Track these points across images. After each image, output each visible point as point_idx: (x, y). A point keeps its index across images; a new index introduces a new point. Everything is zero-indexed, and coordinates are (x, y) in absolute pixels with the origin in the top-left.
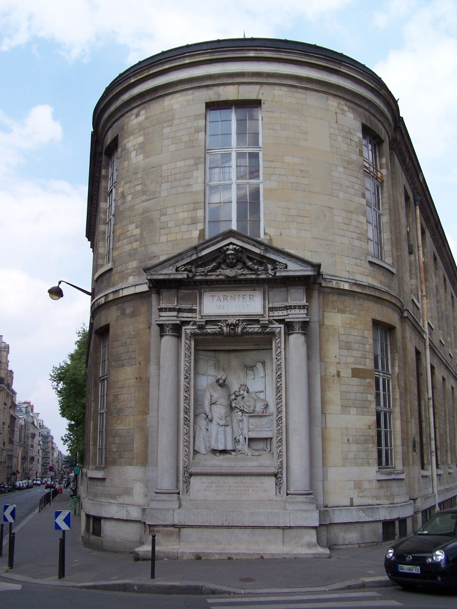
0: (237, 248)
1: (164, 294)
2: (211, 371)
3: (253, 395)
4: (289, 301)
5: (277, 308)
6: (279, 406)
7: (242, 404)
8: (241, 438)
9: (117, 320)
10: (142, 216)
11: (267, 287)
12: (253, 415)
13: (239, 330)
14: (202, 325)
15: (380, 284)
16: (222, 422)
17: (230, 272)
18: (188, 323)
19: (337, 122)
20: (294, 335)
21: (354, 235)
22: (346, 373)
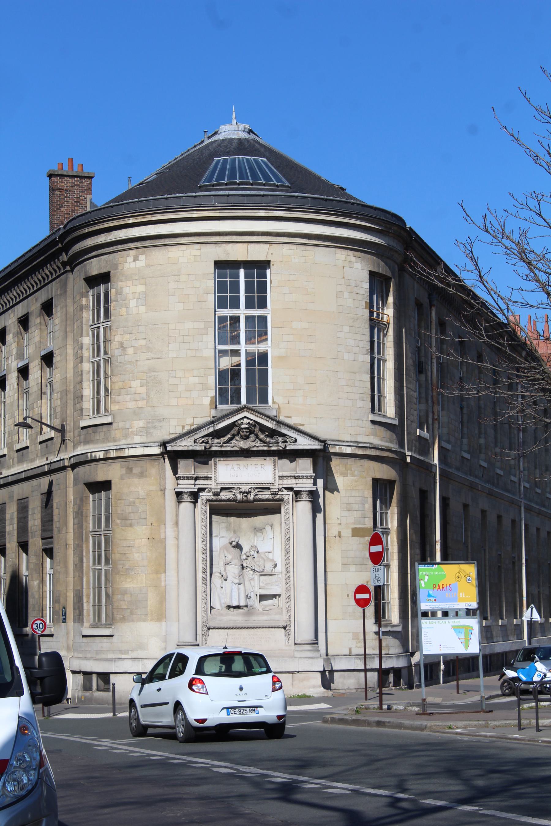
0: (251, 422)
1: (181, 464)
2: (224, 533)
3: (263, 556)
4: (298, 470)
6: (288, 566)
7: (253, 564)
8: (253, 595)
9: (122, 478)
10: (148, 374)
11: (277, 458)
12: (263, 574)
15: (382, 440)
16: (237, 581)
19: (344, 278)
20: (301, 502)
21: (357, 396)
22: (347, 533)
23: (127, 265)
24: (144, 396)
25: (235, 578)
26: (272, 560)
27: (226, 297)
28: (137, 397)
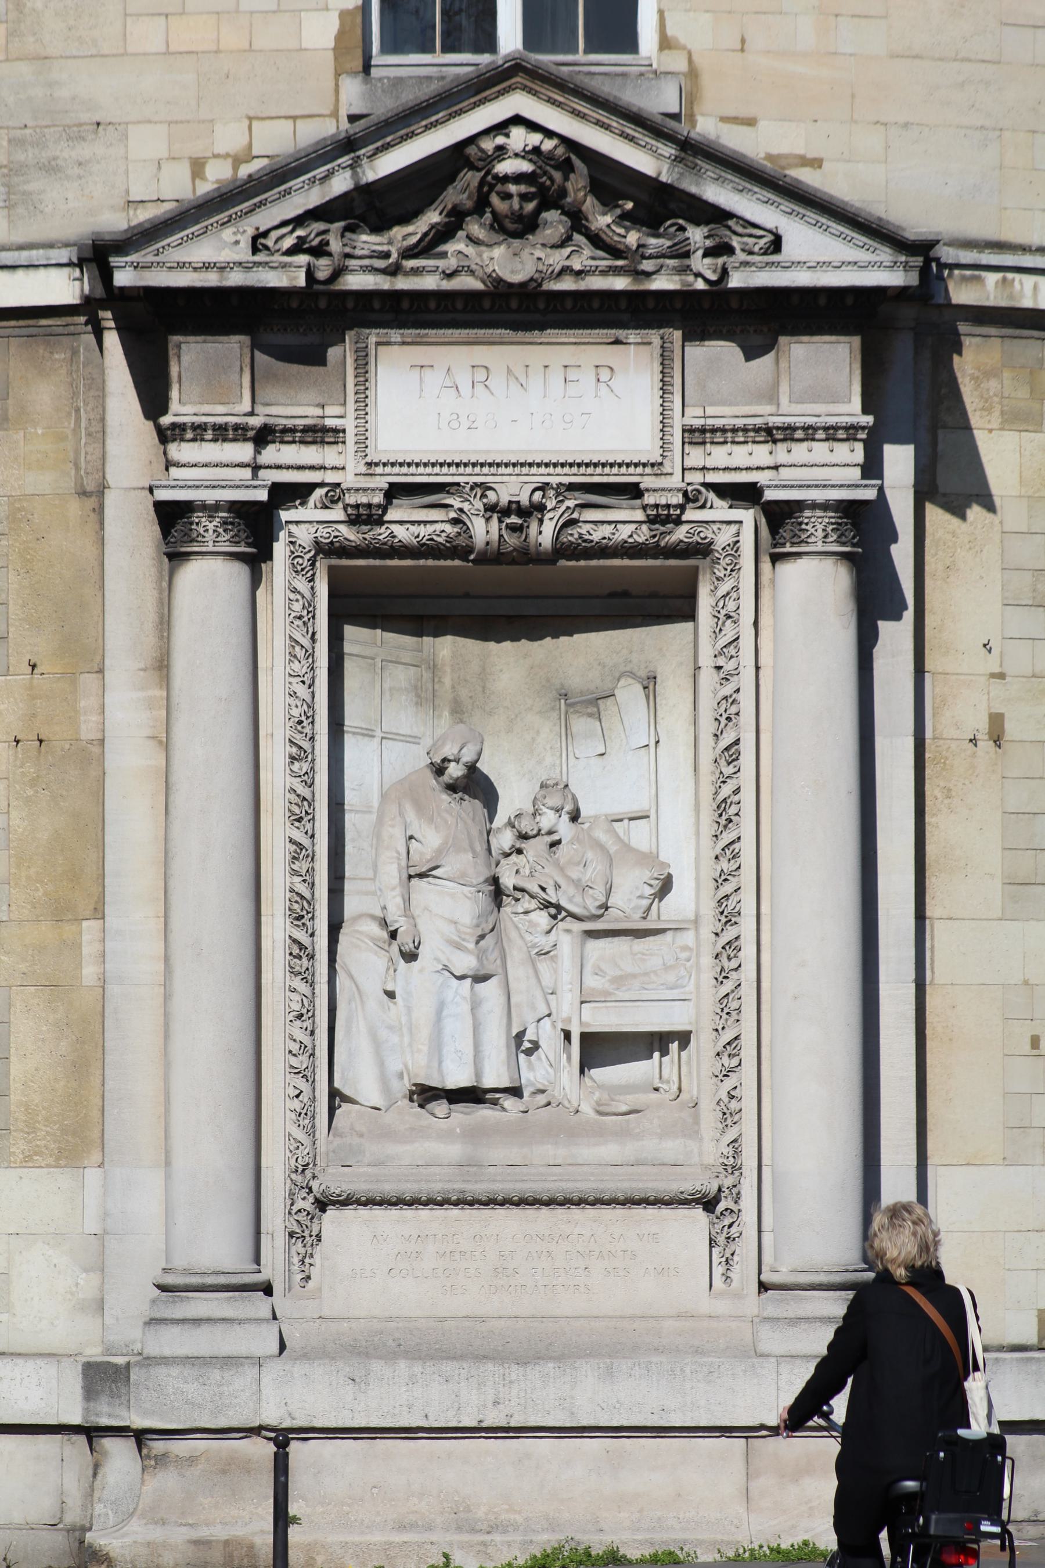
0: (548, 145)
2: (403, 718)
4: (784, 400)
5: (723, 430)
14: (369, 506)
18: (299, 493)
25: (458, 947)
26: (650, 859)
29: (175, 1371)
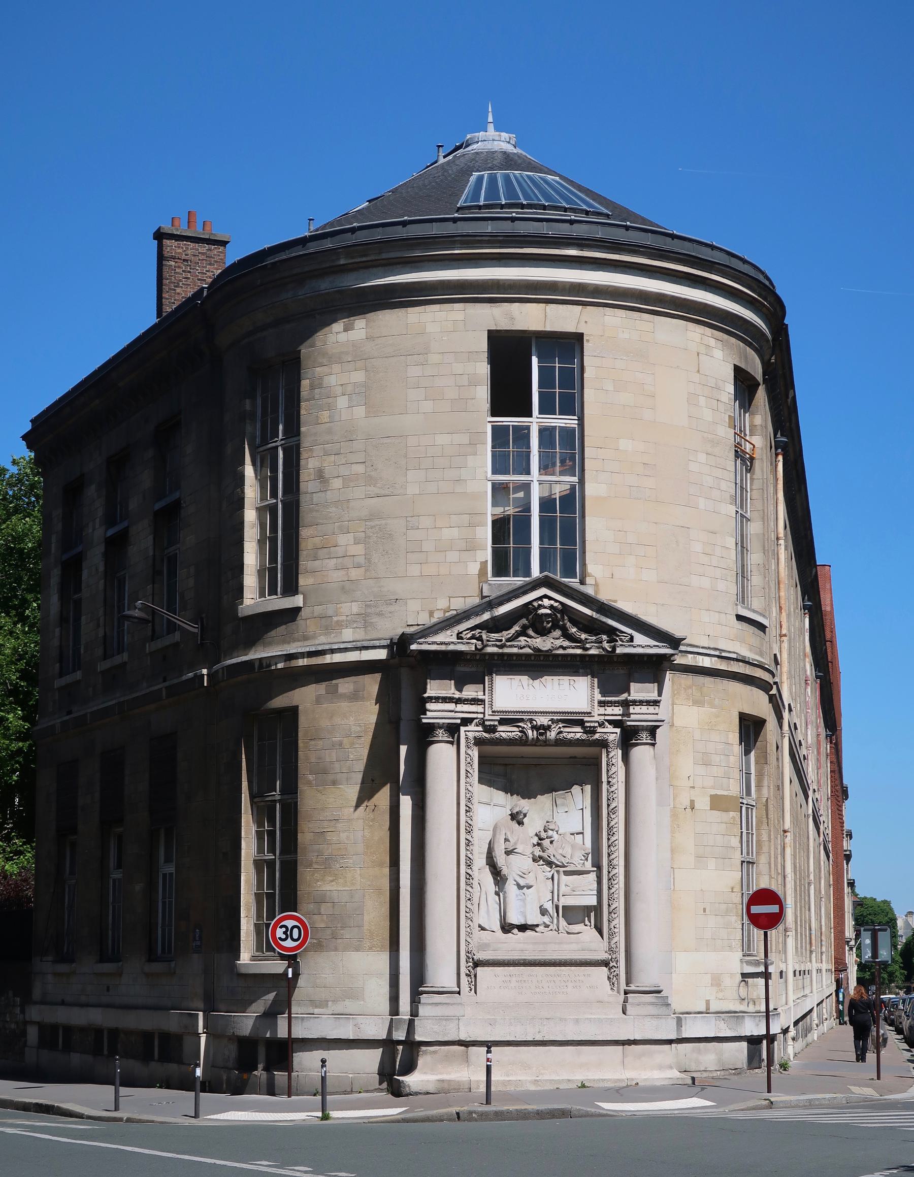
13: (552, 735)
15: (751, 651)
17: (544, 643)
22: (703, 803)
23: (331, 338)
24: (361, 560)
27: (508, 395)
28: (348, 562)
29: (430, 1021)
